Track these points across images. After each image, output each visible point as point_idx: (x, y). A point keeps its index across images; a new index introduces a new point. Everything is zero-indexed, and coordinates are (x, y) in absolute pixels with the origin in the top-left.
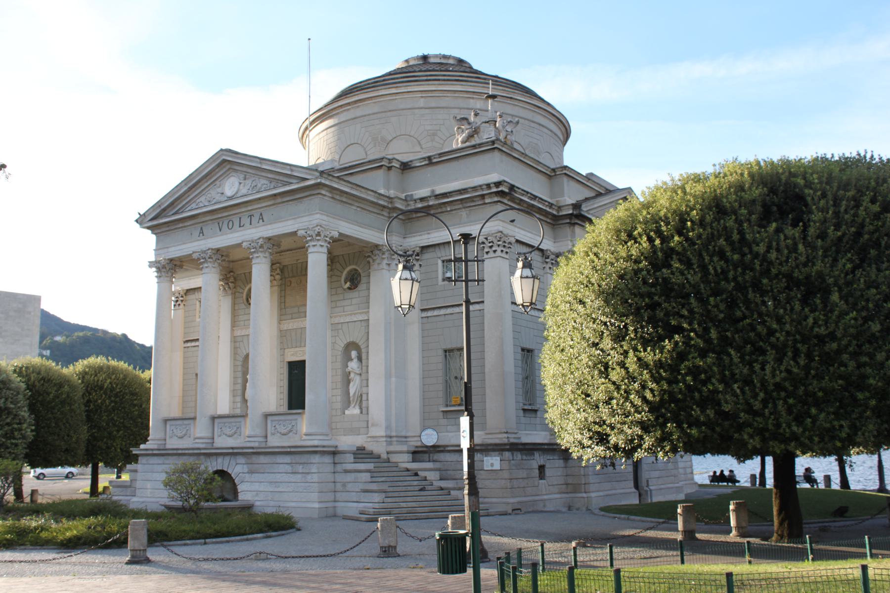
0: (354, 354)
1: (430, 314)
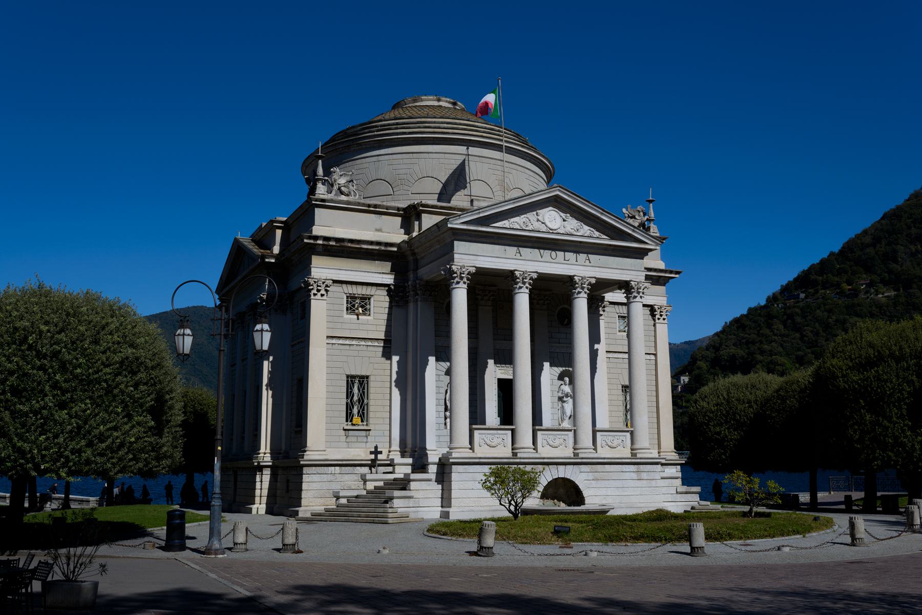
0: (567, 379)
1: (611, 355)
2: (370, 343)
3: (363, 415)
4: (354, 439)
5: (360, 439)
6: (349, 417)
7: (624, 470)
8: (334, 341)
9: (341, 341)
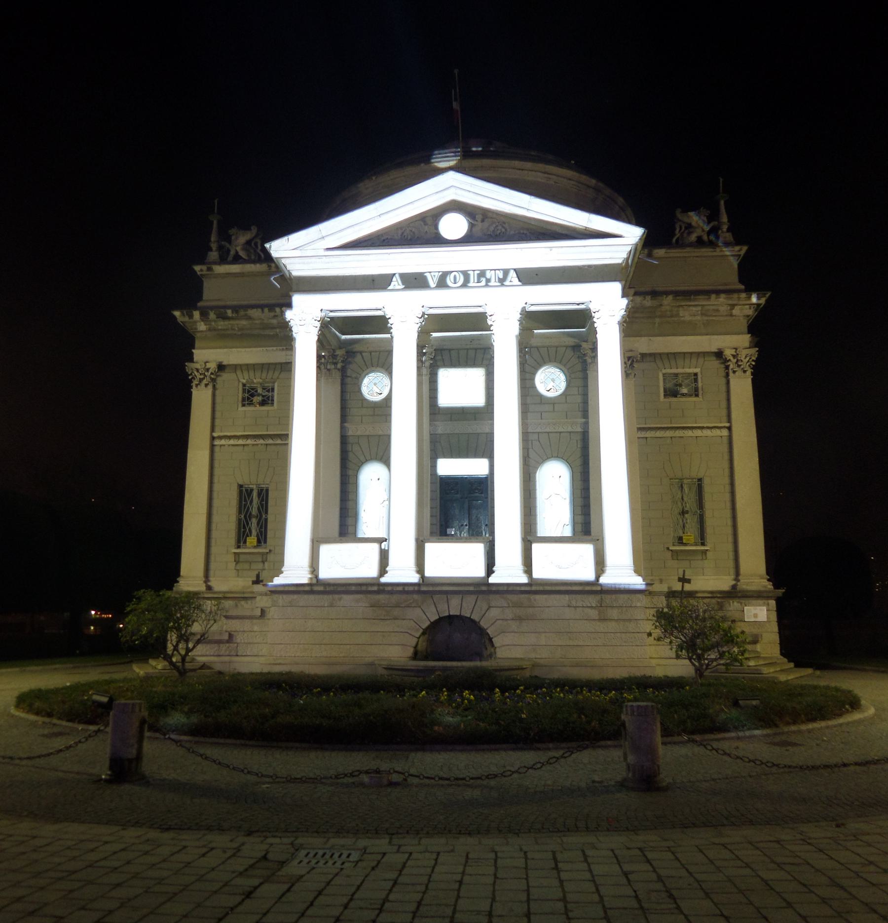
1: (649, 434)
2: (270, 441)
3: (262, 539)
4: (246, 566)
5: (254, 566)
6: (241, 537)
7: (574, 603)
8: (223, 442)
9: (232, 442)
